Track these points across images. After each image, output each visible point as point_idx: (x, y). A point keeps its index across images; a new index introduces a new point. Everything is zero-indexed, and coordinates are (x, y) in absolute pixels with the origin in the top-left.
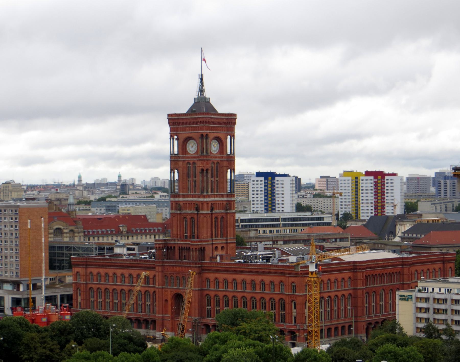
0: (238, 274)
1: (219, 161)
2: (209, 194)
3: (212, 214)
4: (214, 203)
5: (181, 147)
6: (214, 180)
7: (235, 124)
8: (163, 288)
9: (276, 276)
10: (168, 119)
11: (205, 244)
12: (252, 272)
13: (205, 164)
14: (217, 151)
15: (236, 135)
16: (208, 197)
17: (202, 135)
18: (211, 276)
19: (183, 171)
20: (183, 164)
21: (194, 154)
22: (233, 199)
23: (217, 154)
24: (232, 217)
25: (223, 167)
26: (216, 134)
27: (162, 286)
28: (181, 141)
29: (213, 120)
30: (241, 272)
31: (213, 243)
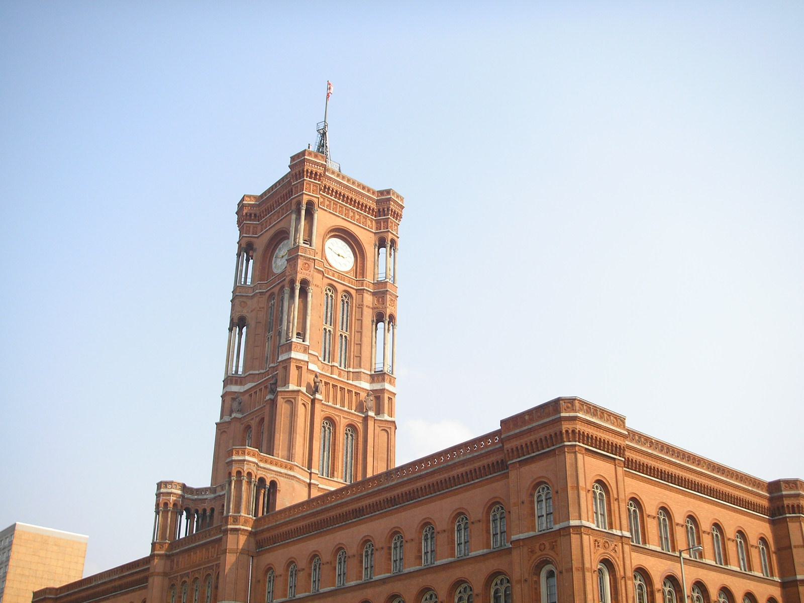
0: (348, 526)
1: (353, 292)
3: (313, 401)
7: (398, 216)
9: (474, 486)
12: (392, 502)
15: (400, 243)
16: (302, 349)
18: (277, 558)
19: (257, 319)
22: (387, 386)
23: (347, 273)
25: (360, 307)
29: (333, 186)
30: (358, 514)
31: (312, 481)
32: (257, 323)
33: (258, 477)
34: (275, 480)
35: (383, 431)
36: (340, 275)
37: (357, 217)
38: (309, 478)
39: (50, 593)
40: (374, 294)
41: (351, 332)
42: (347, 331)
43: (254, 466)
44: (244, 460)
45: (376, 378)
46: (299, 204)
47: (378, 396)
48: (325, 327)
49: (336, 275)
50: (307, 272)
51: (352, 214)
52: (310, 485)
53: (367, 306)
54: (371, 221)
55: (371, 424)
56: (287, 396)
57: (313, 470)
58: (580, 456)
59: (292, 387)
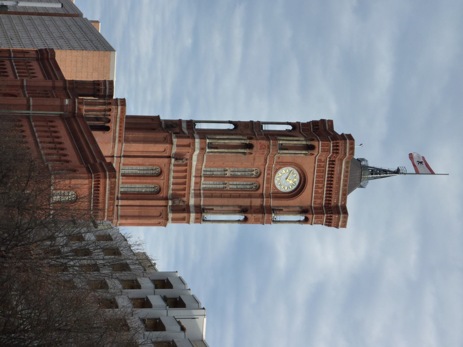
1: (260, 191)
3: (169, 157)
7: (329, 223)
8: (22, 87)
11: (115, 133)
14: (278, 187)
15: (307, 226)
16: (202, 147)
22: (193, 216)
23: (274, 186)
24: (159, 214)
25: (250, 196)
26: (312, 178)
27: (26, 86)
29: (337, 168)
31: (115, 158)
33: (110, 117)
34: (111, 130)
35: (160, 214)
36: (270, 180)
38: (117, 156)
39: (51, 55)
40: (262, 206)
43: (115, 113)
44: (117, 106)
46: (312, 140)
47: (186, 209)
49: (269, 176)
50: (259, 147)
51: (320, 186)
52: (113, 157)
53: (251, 201)
55: (162, 203)
56: (168, 138)
57: (122, 158)
58: (86, 181)
59: (175, 140)
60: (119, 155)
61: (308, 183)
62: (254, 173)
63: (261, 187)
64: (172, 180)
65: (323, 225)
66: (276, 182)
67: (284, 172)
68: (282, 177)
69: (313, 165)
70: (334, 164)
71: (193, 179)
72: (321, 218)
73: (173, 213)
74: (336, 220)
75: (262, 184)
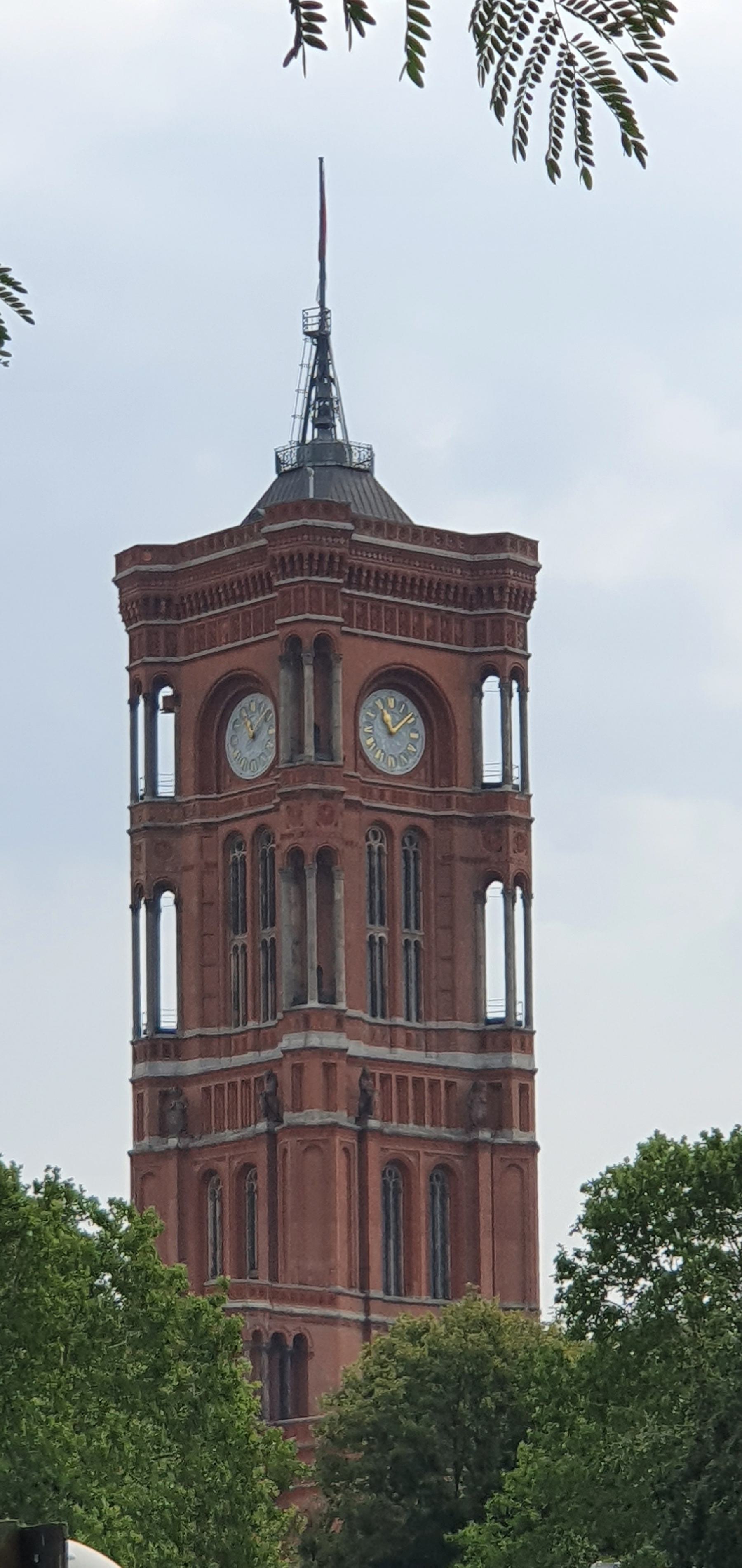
1: (426, 825)
2: (342, 1005)
3: (362, 1135)
4: (385, 1078)
5: (190, 748)
6: (392, 934)
10: (116, 582)
13: (310, 813)
14: (412, 763)
17: (294, 642)
20: (201, 849)
21: (266, 775)
22: (517, 1060)
23: (409, 776)
26: (394, 647)
28: (194, 703)
29: (371, 562)
31: (374, 1317)
32: (202, 905)
37: (427, 622)
41: (427, 931)
42: (417, 927)
45: (489, 1041)
48: (371, 933)
49: (388, 794)
50: (330, 828)
53: (462, 858)
54: (462, 623)
60: (360, 1303)
61: (408, 661)
62: (376, 845)
63: (417, 821)
64: (411, 1128)
65: (527, 619)
66: (398, 770)
67: (371, 740)
68: (384, 747)
69: (359, 641)
70: (360, 570)
71: (401, 1054)
72: (512, 623)
73: (511, 1127)
74: (520, 574)
75: (409, 817)
